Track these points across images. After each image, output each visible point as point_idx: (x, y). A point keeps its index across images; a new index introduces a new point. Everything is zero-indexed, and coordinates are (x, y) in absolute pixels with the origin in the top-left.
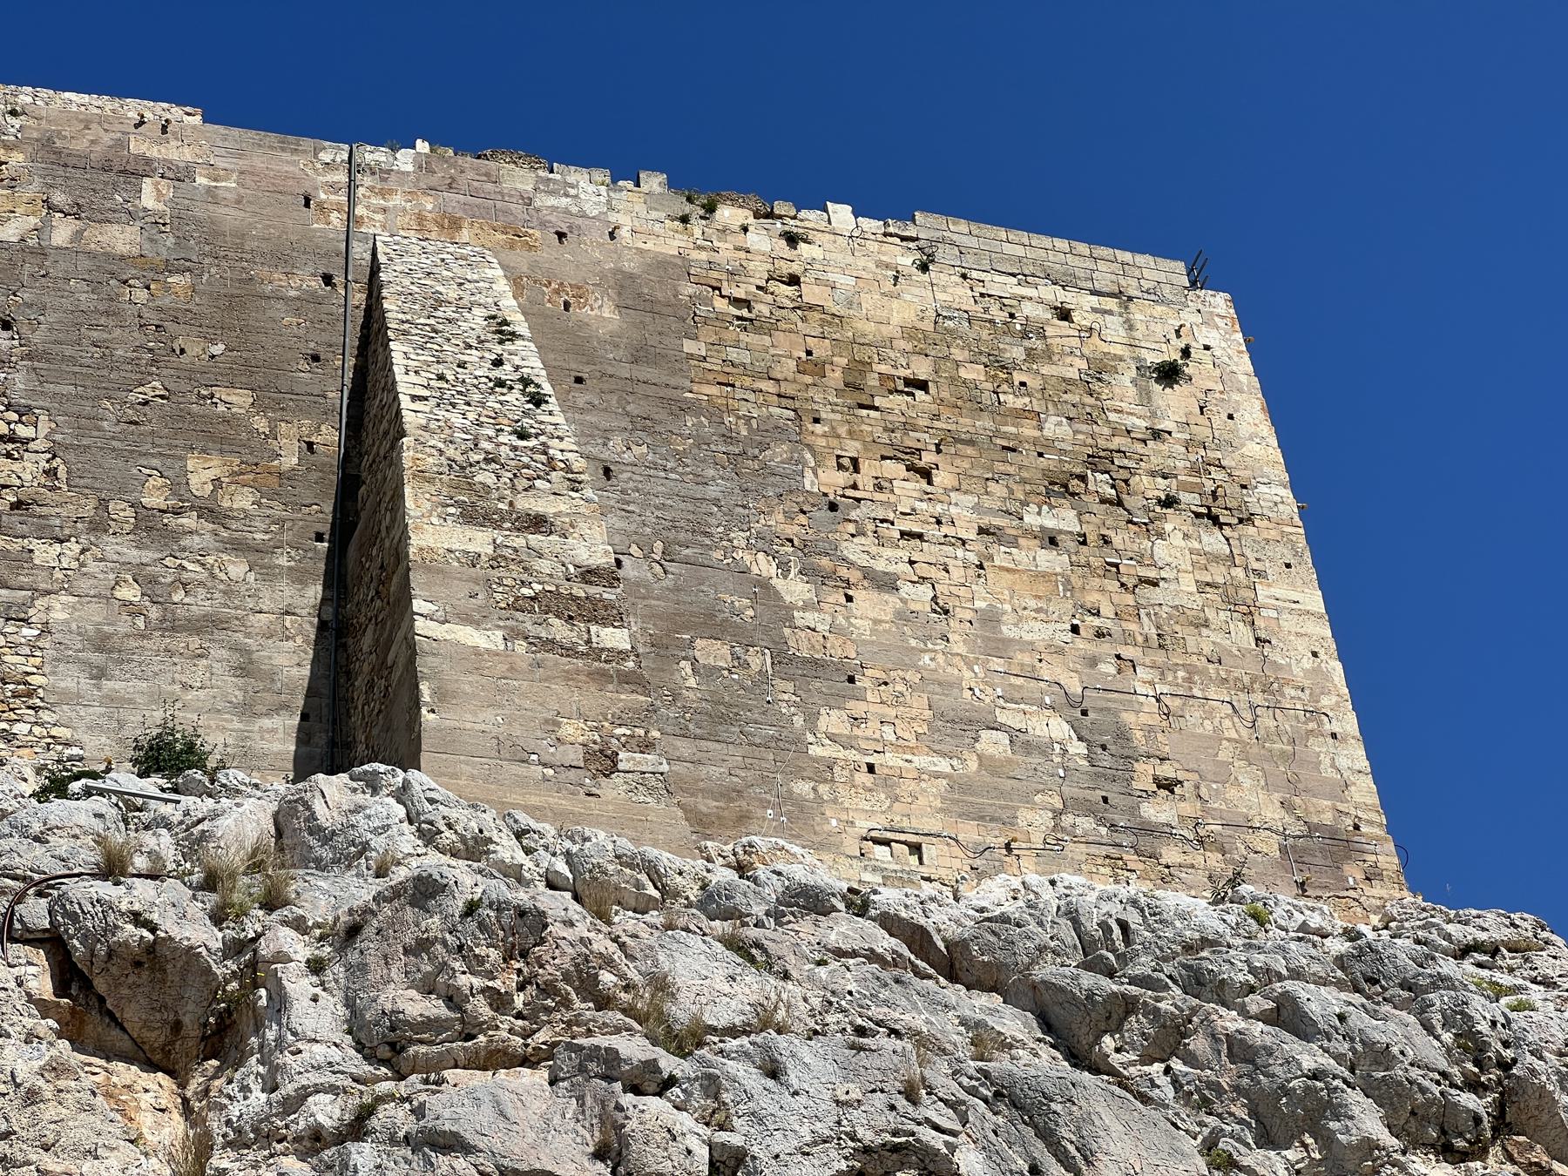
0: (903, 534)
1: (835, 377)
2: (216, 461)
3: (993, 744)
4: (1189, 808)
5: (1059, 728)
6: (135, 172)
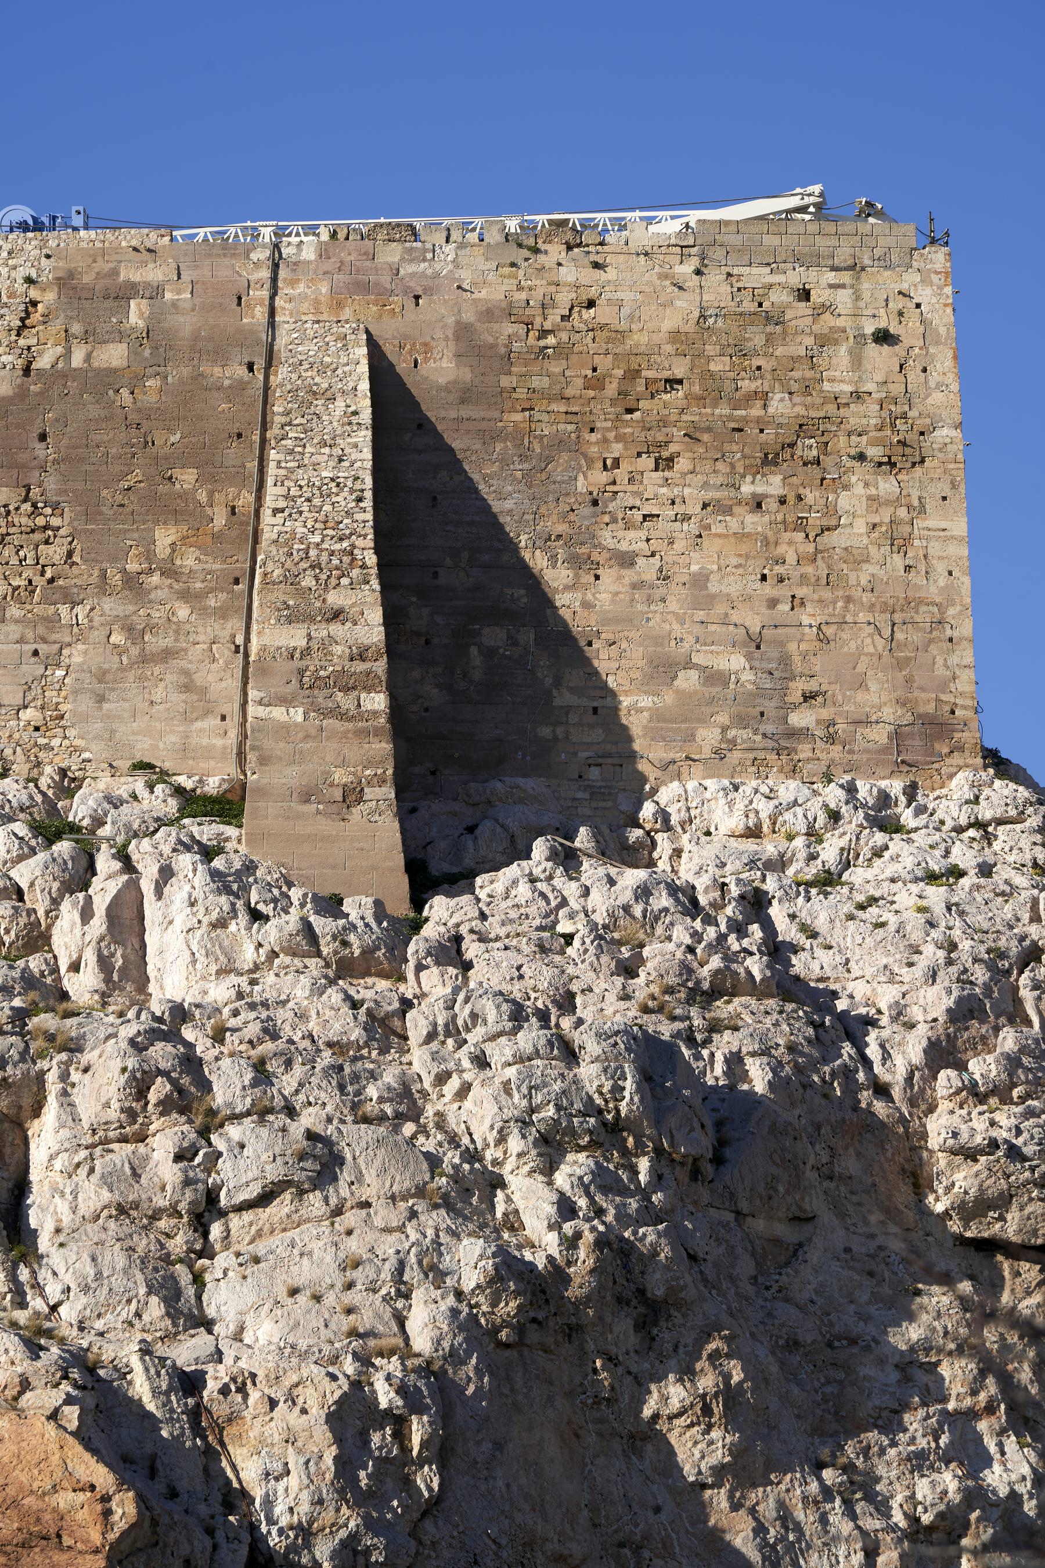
0: (645, 516)
1: (612, 389)
2: (173, 530)
3: (688, 680)
4: (825, 713)
5: (736, 662)
6: (124, 294)
